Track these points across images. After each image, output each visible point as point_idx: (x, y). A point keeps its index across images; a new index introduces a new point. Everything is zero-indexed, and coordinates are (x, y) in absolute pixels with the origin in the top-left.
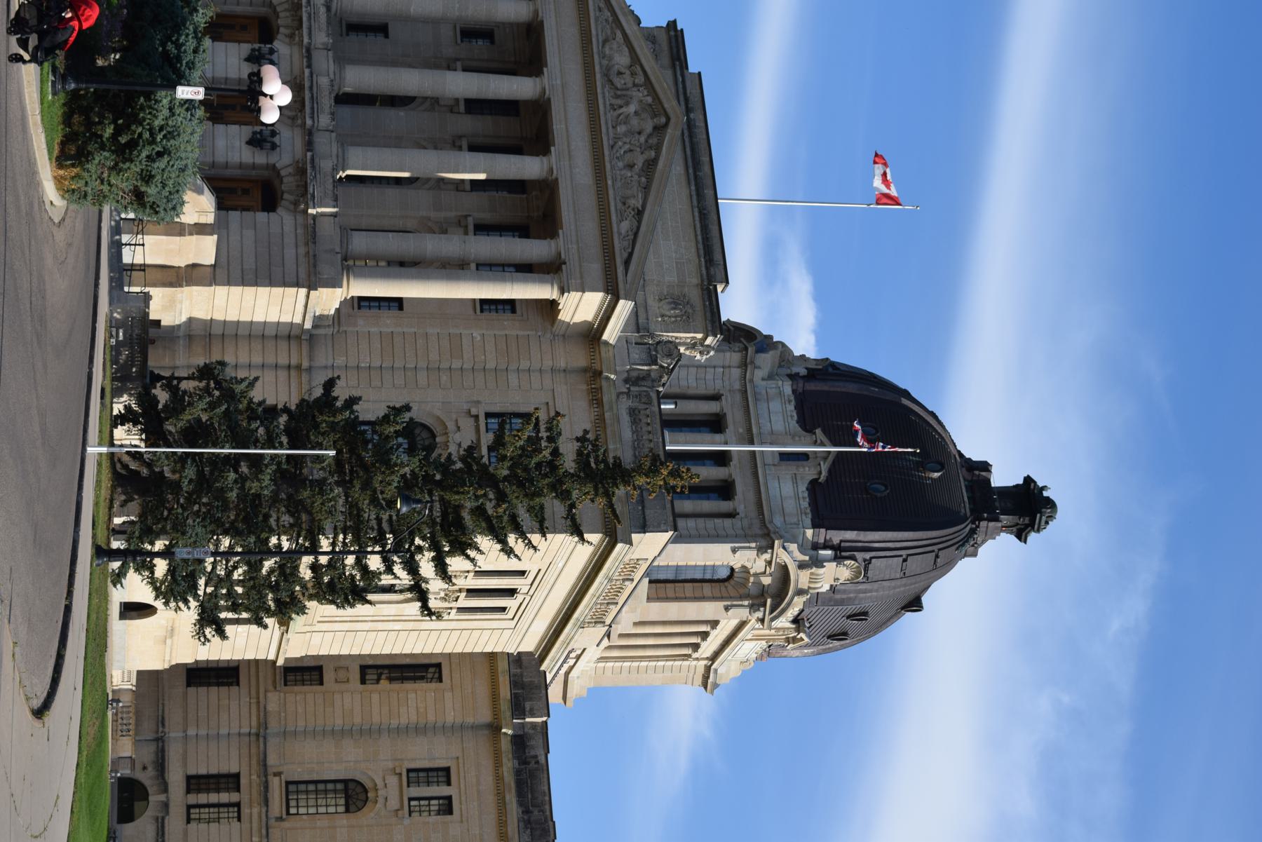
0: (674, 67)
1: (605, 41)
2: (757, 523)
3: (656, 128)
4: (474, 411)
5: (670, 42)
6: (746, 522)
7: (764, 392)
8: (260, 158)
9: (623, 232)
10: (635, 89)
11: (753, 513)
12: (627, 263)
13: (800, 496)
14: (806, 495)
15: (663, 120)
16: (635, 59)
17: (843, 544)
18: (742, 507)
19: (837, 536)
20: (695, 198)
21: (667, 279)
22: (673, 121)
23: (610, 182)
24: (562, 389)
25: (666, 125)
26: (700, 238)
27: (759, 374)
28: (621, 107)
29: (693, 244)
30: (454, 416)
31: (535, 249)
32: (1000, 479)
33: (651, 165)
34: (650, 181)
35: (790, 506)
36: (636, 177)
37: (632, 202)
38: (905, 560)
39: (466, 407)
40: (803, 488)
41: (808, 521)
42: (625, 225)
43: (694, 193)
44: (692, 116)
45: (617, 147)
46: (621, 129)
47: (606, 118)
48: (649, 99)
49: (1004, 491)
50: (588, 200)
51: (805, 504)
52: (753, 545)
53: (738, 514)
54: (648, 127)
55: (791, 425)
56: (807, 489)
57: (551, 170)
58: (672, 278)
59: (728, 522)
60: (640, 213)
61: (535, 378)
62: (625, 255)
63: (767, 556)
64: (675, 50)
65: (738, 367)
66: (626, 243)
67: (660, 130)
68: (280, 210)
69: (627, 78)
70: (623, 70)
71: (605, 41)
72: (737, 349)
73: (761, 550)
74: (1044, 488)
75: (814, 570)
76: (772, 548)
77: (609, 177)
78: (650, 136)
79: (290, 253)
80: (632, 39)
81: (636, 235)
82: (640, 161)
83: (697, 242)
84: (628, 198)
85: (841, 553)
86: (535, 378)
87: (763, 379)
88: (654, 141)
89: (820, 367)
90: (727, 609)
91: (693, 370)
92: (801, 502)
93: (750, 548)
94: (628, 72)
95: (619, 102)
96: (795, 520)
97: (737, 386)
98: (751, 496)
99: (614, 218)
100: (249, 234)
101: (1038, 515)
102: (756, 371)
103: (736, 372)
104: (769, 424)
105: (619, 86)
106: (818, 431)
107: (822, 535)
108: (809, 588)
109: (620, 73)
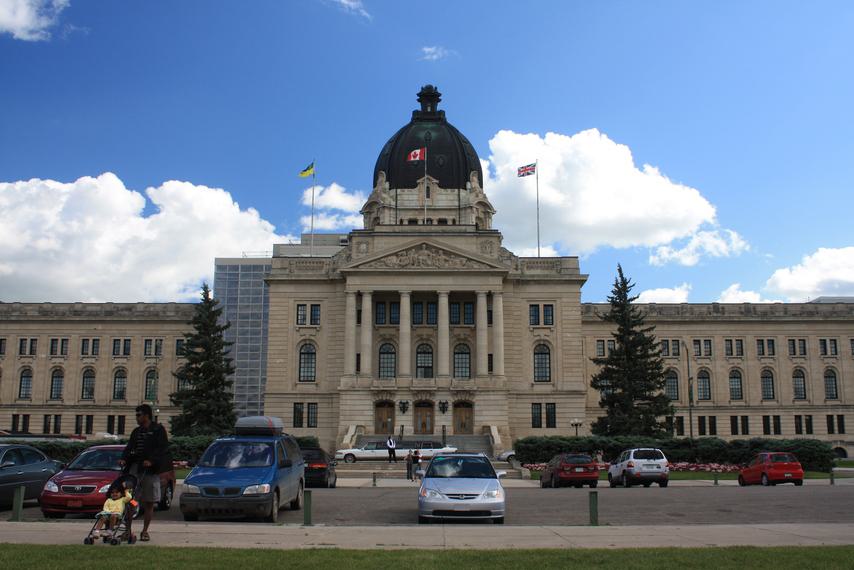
8: (450, 408)
16: (396, 254)
25: (427, 244)
31: (482, 303)
32: (418, 107)
33: (445, 252)
34: (454, 254)
47: (424, 268)
49: (424, 107)
58: (475, 247)
60: (469, 260)
67: (429, 247)
68: (474, 400)
74: (422, 88)
79: (492, 397)
100: (484, 413)
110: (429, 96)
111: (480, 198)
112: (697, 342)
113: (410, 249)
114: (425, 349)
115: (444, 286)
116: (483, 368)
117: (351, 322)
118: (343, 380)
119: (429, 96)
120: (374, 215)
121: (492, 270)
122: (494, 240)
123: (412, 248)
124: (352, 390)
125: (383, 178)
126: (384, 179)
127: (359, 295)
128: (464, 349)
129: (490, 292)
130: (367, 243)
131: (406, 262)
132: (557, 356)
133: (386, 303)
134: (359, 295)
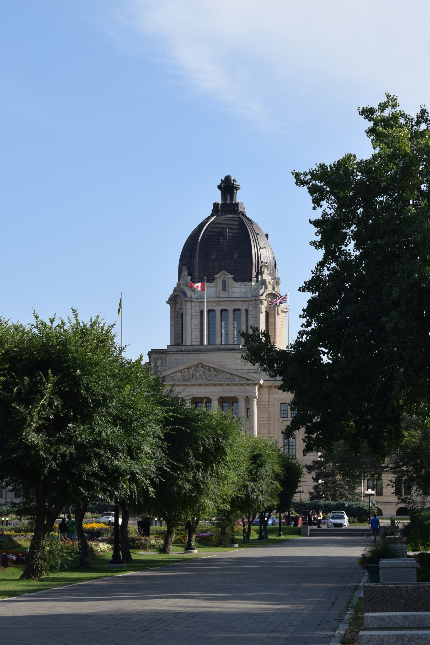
0: (166, 354)
1: (174, 380)
2: (251, 303)
3: (202, 367)
4: (282, 421)
5: (157, 354)
6: (250, 306)
7: (199, 294)
9: (238, 380)
10: (190, 372)
11: (247, 303)
12: (248, 380)
13: (239, 285)
14: (239, 283)
15: (200, 365)
16: (180, 371)
17: (257, 271)
18: (244, 307)
19: (254, 274)
20: (212, 352)
21: (240, 363)
22: (201, 362)
23: (223, 383)
24: (274, 396)
26: (226, 352)
27: (194, 296)
28: (197, 377)
29: (228, 354)
30: (283, 426)
31: (242, 404)
32: (218, 198)
35: (243, 289)
36: (220, 374)
37: (229, 376)
38: (261, 248)
39: (280, 423)
40: (236, 284)
41: (249, 284)
42: (236, 379)
43: (211, 352)
44: (183, 350)
45: (210, 379)
46: (204, 378)
48: (193, 368)
49: (224, 198)
50: (226, 388)
51: (243, 284)
52: (260, 306)
53: (247, 309)
54: (202, 369)
55: (212, 285)
56: (237, 282)
57: (217, 398)
59: (250, 313)
60: (232, 374)
61: (271, 403)
62: (245, 380)
63: (264, 301)
64: (160, 353)
65: (191, 303)
66: (242, 379)
69: (185, 374)
70: (182, 375)
71: (174, 380)
72: (185, 304)
73: (262, 303)
75: (267, 283)
76: (261, 299)
77: (221, 383)
78: (205, 369)
80: (173, 372)
81: (239, 376)
82: (213, 373)
83: (228, 353)
84: (226, 377)
85: (260, 272)
86: (271, 403)
87: (195, 294)
88: (207, 368)
89: (187, 271)
90: (278, 314)
91: (193, 320)
92: (242, 285)
93: (261, 307)
94: (184, 374)
95: (195, 378)
96: (249, 288)
97: (198, 304)
98: (240, 303)
99: (234, 382)
101: (235, 186)
102: (193, 297)
103: (193, 304)
104: (212, 294)
105: (189, 377)
106: (215, 276)
107: (254, 279)
108: (272, 285)
109: (184, 376)
111: (270, 290)
113: (191, 367)
120: (178, 306)
121: (248, 382)
123: (192, 366)
125: (185, 273)
126: (186, 274)
129: (247, 397)
130: (161, 359)
131: (188, 377)
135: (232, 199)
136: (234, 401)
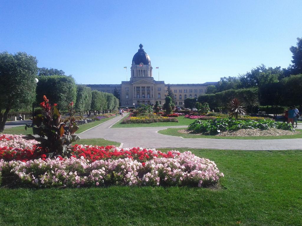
49: (140, 48)
110: (141, 46)
112: (185, 90)
114: (143, 93)
115: (146, 85)
116: (151, 97)
117: (134, 90)
118: (133, 99)
119: (141, 46)
122: (152, 78)
124: (134, 99)
127: (135, 87)
128: (149, 93)
132: (161, 94)
133: (138, 88)
134: (135, 87)
135: (142, 49)
136: (150, 87)
